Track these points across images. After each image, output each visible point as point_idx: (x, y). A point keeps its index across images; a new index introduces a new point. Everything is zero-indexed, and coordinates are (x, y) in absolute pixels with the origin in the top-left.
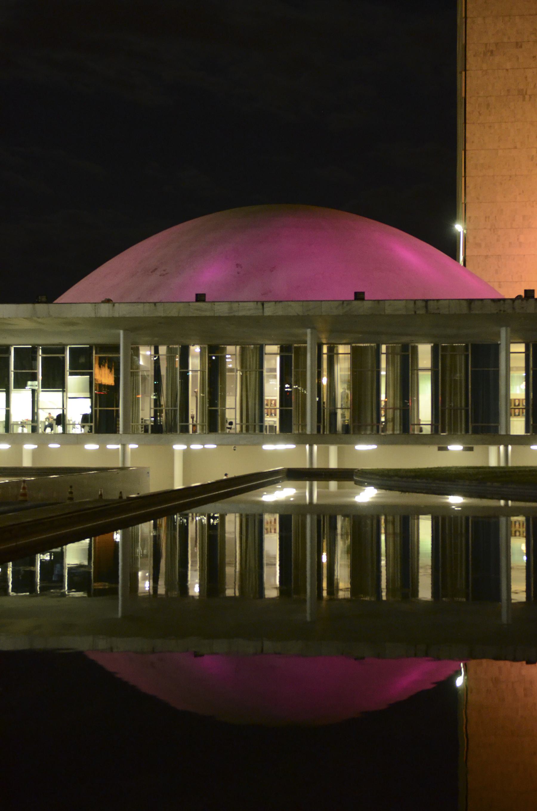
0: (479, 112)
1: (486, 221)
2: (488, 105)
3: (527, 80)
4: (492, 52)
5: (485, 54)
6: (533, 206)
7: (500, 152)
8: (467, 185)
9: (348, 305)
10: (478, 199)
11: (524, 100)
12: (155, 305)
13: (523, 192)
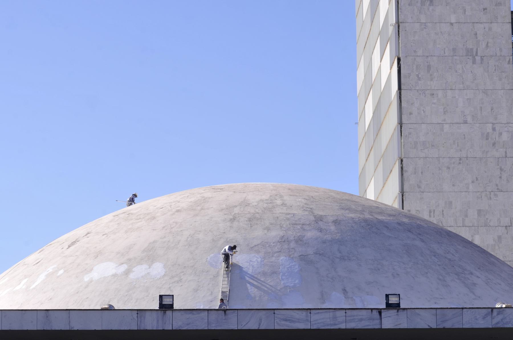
0: (418, 76)
2: (429, 67)
3: (477, 38)
6: (490, 198)
7: (446, 127)
8: (404, 169)
9: (498, 314)
10: (419, 187)
11: (474, 62)
12: (225, 312)
13: (477, 179)
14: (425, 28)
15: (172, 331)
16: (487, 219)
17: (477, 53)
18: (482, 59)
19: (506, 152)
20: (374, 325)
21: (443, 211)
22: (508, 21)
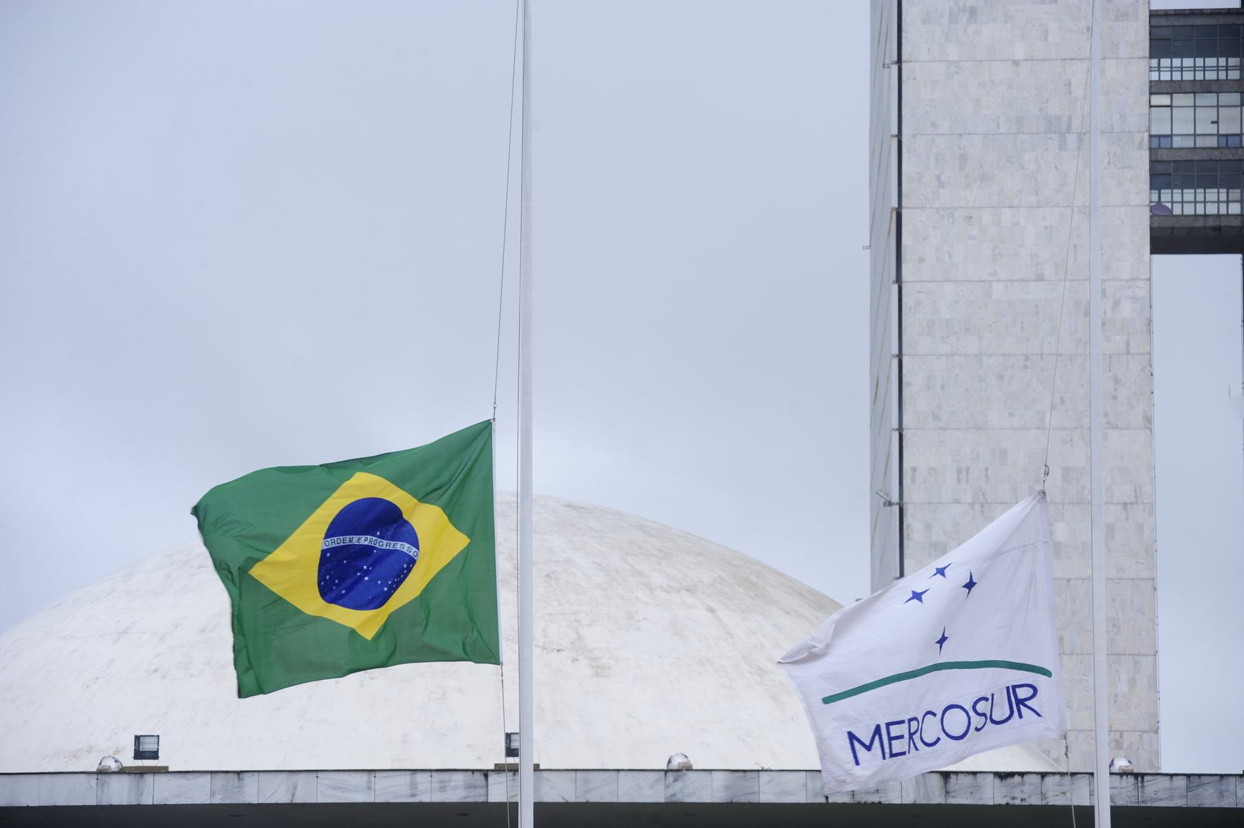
0: (938, 178)
1: (959, 480)
2: (963, 159)
3: (1070, 93)
4: (973, 12)
5: (953, 19)
7: (998, 290)
8: (904, 380)
10: (936, 418)
11: (1062, 147)
13: (1062, 401)
14: (957, 73)
15: (153, 805)
16: (1083, 487)
17: (1069, 125)
18: (1080, 140)
19: (1128, 344)
20: (475, 796)
21: (987, 470)
22: (1141, 54)
